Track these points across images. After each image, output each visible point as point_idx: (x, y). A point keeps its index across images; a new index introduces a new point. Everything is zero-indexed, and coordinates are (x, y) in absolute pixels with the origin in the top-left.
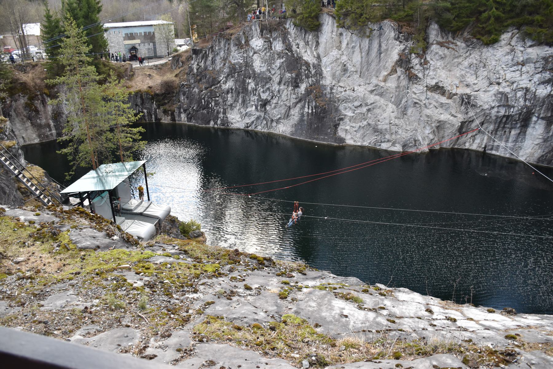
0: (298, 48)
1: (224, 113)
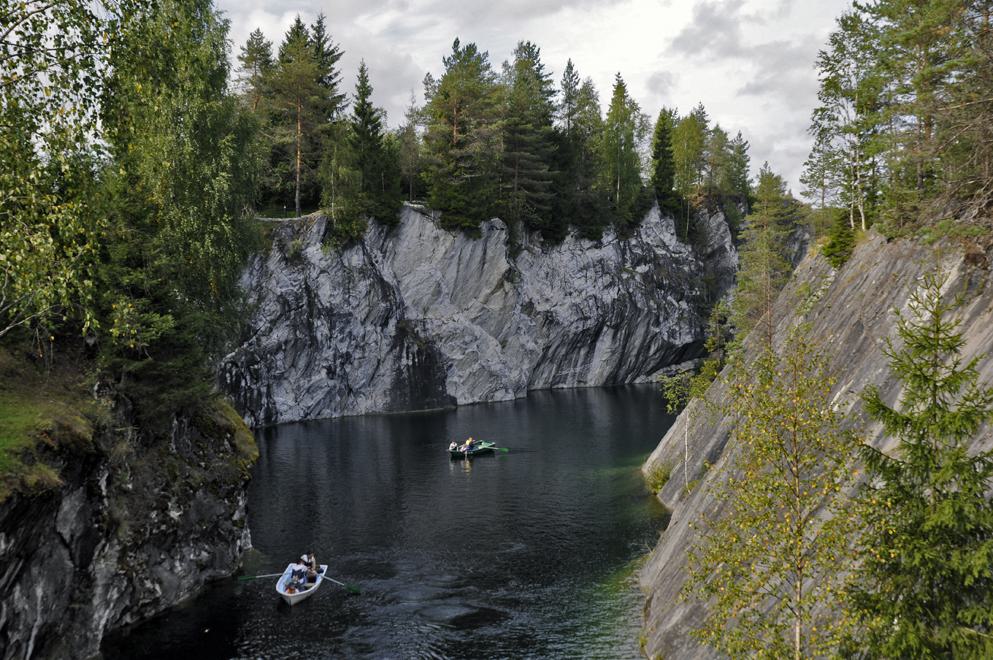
1: (269, 395)
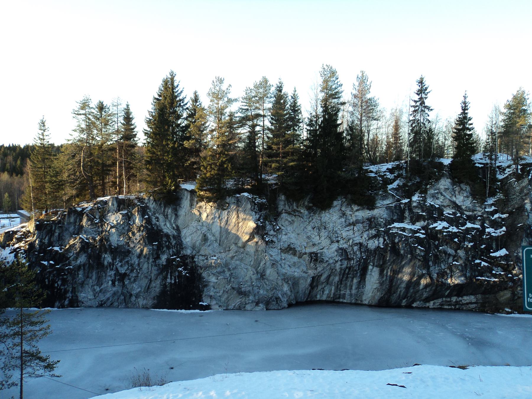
0: (158, 221)
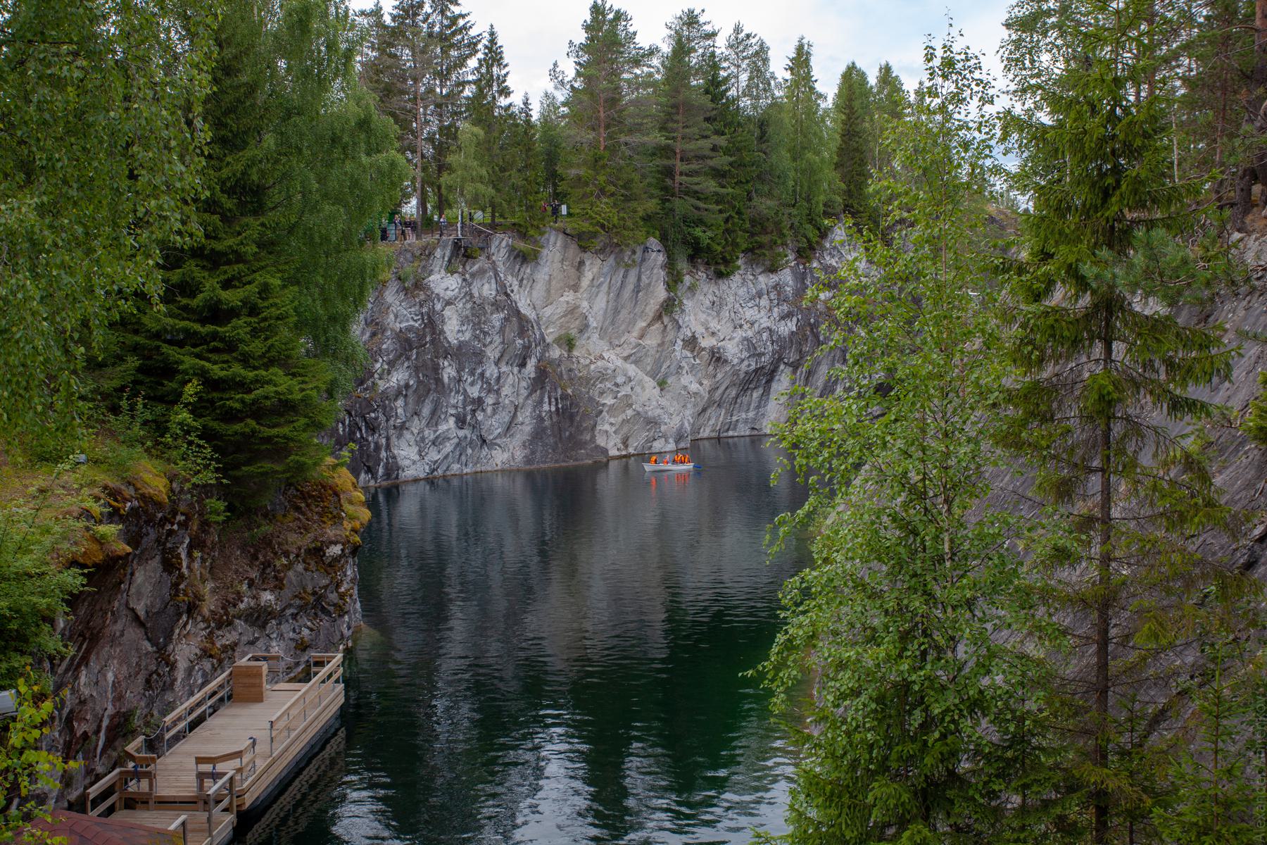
1: (388, 447)
